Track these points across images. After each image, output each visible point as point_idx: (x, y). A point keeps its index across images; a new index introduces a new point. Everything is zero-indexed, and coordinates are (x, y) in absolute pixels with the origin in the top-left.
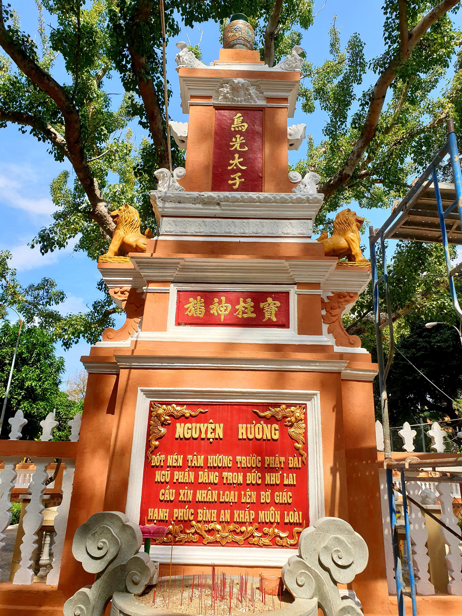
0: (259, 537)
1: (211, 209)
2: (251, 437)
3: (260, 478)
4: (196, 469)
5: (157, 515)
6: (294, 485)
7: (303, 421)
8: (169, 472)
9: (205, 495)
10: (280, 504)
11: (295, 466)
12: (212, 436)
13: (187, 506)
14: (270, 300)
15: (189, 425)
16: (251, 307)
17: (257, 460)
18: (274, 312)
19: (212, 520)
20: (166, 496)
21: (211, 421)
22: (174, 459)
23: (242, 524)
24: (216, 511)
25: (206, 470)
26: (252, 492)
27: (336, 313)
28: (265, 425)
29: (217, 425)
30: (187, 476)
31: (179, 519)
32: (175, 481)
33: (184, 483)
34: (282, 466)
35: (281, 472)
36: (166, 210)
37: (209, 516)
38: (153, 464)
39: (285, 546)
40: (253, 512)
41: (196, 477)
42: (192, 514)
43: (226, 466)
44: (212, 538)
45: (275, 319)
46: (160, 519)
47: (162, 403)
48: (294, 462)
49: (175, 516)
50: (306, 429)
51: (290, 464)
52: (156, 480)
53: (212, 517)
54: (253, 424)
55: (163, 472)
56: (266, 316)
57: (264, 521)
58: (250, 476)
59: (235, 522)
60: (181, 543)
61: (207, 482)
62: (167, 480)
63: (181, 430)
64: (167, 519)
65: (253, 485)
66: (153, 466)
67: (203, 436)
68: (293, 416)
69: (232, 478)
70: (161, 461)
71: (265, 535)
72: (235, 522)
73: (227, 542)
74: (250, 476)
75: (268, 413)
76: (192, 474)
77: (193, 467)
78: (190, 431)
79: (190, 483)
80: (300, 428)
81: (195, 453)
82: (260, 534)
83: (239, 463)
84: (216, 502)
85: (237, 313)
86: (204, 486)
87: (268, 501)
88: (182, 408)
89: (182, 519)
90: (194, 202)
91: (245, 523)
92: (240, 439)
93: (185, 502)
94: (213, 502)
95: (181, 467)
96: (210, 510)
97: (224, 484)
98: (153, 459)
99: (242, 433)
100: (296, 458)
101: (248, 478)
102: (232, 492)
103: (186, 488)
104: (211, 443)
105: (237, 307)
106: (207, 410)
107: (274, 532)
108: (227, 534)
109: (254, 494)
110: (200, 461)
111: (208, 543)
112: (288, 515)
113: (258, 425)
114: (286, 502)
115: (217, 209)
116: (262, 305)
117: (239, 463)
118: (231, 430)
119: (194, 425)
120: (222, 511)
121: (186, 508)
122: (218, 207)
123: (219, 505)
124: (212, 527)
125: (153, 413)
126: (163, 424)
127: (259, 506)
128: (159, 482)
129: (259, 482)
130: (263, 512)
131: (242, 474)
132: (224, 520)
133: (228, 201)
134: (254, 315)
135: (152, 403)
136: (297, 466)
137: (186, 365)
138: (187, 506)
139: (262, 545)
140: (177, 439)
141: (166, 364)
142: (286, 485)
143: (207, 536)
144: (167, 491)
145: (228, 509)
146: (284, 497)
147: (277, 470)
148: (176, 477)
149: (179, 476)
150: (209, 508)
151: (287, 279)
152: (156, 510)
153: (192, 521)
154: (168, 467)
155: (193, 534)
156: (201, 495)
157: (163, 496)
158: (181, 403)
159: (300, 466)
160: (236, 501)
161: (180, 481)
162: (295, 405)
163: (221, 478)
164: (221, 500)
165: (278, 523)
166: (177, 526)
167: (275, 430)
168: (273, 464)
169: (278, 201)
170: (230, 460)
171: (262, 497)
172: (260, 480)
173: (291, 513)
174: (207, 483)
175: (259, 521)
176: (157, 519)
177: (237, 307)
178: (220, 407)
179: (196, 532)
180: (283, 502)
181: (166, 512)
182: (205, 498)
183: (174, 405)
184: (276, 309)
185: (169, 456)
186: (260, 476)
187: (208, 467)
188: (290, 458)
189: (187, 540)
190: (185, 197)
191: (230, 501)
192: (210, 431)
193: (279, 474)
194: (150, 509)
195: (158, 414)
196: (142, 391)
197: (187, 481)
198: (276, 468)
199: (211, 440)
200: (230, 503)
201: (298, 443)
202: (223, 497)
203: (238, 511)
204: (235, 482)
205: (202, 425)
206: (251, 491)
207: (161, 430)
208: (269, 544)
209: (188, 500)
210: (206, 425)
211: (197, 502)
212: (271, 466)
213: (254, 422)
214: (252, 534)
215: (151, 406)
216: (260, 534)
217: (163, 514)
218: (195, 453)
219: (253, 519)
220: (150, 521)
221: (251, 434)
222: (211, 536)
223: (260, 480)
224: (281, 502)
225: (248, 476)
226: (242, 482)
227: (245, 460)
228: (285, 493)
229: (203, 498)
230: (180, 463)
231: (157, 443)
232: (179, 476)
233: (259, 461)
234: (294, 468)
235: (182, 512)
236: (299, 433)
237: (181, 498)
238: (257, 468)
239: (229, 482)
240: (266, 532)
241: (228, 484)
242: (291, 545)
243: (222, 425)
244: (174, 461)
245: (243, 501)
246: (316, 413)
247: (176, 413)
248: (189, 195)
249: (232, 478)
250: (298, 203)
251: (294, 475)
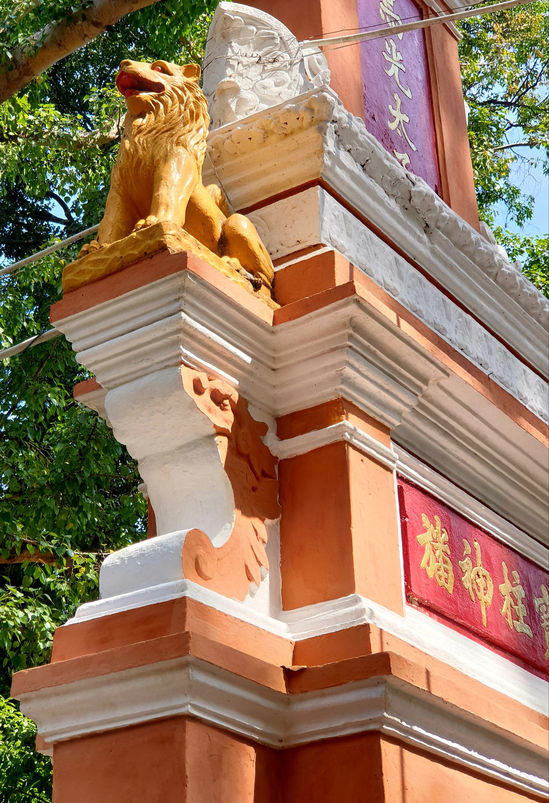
1: (414, 234)
36: (338, 170)
90: (389, 189)
122: (425, 237)
133: (448, 234)
190: (380, 161)
248: (388, 159)
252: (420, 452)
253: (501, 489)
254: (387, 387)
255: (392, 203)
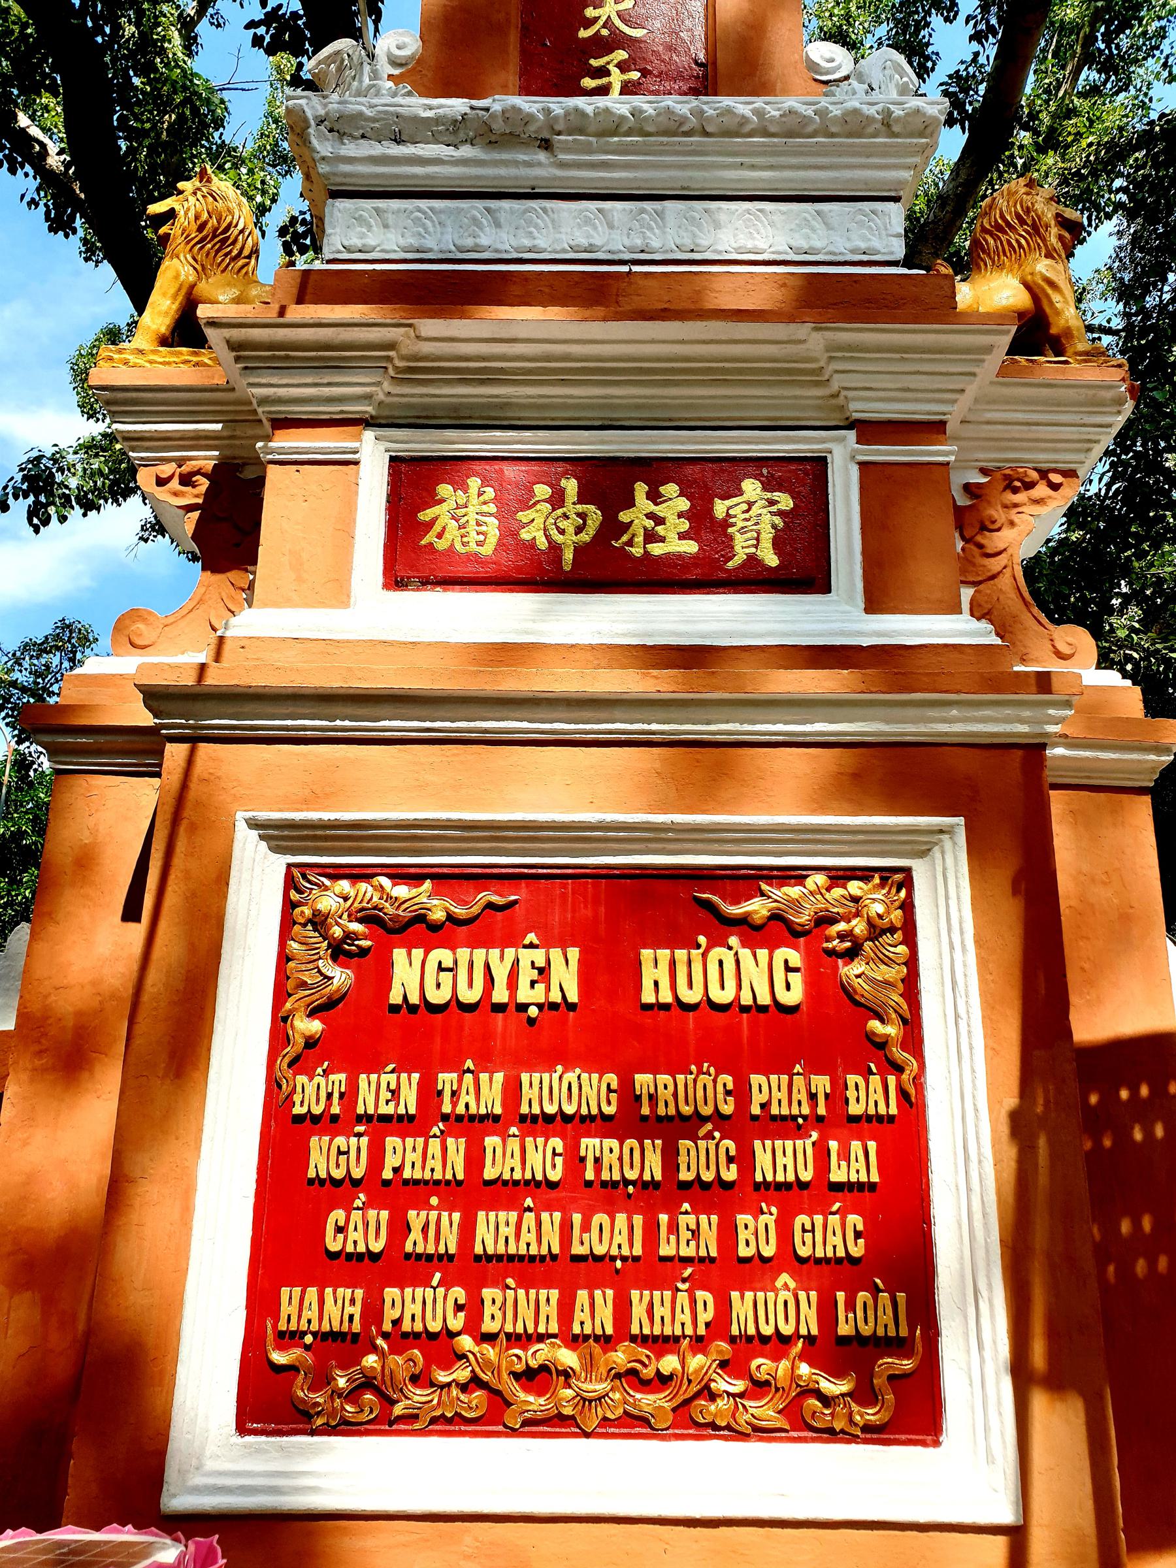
0: (734, 1395)
1: (516, 163)
2: (692, 996)
3: (730, 1160)
4: (474, 1126)
5: (313, 1314)
6: (872, 1186)
7: (899, 936)
8: (364, 1140)
9: (510, 1231)
10: (818, 1261)
11: (871, 1111)
12: (538, 994)
13: (438, 1276)
14: (751, 488)
15: (442, 955)
16: (680, 515)
17: (720, 1089)
18: (767, 536)
19: (541, 1329)
20: (352, 1235)
21: (531, 937)
22: (386, 1090)
23: (663, 1344)
24: (555, 1294)
25: (514, 1130)
26: (703, 1218)
27: (1001, 546)
28: (745, 954)
29: (556, 954)
30: (438, 1155)
31: (406, 1326)
32: (387, 1174)
33: (426, 1182)
34: (822, 1110)
35: (815, 1135)
37: (526, 1313)
38: (298, 1110)
39: (842, 1431)
40: (709, 1297)
41: (475, 1159)
42: (459, 1308)
43: (594, 1111)
44: (542, 1401)
45: (772, 560)
46: (326, 1327)
47: (336, 873)
48: (868, 1095)
49: (390, 1314)
50: (912, 963)
51: (852, 1101)
52: (311, 1174)
53: (542, 1318)
54: (699, 946)
55: (340, 1141)
56: (738, 548)
57: (751, 1331)
58: (693, 1153)
59: (633, 1339)
60: (417, 1426)
61: (517, 1176)
62: (358, 1173)
63: (411, 974)
64: (357, 1327)
65: (705, 1186)
66: (299, 1119)
67: (500, 995)
68: (857, 914)
69: (620, 1159)
70: (330, 1096)
71: (759, 1388)
72: (633, 1339)
73: (605, 1419)
74: (693, 1153)
75: (757, 908)
76: (457, 1149)
77: (459, 1118)
78: (446, 977)
79: (448, 1182)
80: (888, 962)
81: (469, 1064)
82: (739, 1386)
83: (645, 1100)
84: (554, 1257)
85: (625, 538)
86: (506, 1193)
87: (769, 1251)
88: (415, 892)
89: (419, 1327)
90: (451, 139)
91: (677, 1339)
92: (648, 1007)
93: (429, 1257)
94: (543, 1258)
95: (411, 1118)
96: (532, 1292)
97: (589, 1184)
98: (299, 1089)
99: (656, 983)
100: (875, 1080)
101: (682, 1160)
102: (621, 1218)
103: (434, 1201)
104: (531, 1021)
105: (624, 517)
106: (513, 898)
107: (794, 1377)
108: (601, 1387)
109: (709, 1224)
110: (486, 1093)
111: (525, 1423)
112: (850, 1306)
113: (717, 952)
114: (841, 1253)
115: (540, 164)
116: (720, 508)
117: (645, 1100)
118: (609, 971)
119: (463, 953)
120: (582, 1295)
121: (435, 1283)
122: (542, 156)
123: (565, 1271)
124: (541, 1358)
125: (298, 910)
126: (338, 952)
127: (728, 1272)
128: (322, 1182)
129: (731, 1174)
130: (749, 1295)
131: (658, 1142)
132: (588, 1330)
133: (581, 132)
134: (690, 547)
135: (296, 872)
136: (882, 1110)
137: (428, 724)
138: (438, 1276)
139: (749, 1430)
140: (395, 1008)
141: (347, 723)
142: (838, 1187)
143: (522, 1396)
144: (356, 1216)
145: (602, 1285)
146: (834, 1234)
147: (799, 1127)
148: (391, 1161)
149: (404, 1156)
150: (526, 1283)
151: (819, 408)
152: (312, 1292)
153: (459, 1334)
154: (360, 1119)
155: (464, 1388)
156: (494, 1231)
157: (341, 1236)
158: (412, 870)
159: (894, 1110)
160: (638, 1251)
161: (407, 1174)
162: (863, 874)
163: (575, 1161)
164: (577, 1249)
165: (809, 1339)
166: (400, 1354)
167: (788, 969)
168: (785, 1103)
169: (772, 129)
170: (609, 1090)
171: (743, 1235)
172: (733, 1167)
173: (863, 1296)
174: (516, 1183)
175: (735, 1331)
176: (314, 1327)
177: (624, 517)
178: (565, 886)
179: (475, 1382)
180: (830, 1254)
181: (353, 1302)
182: (512, 1240)
183: (385, 882)
184: (778, 520)
185: (363, 1077)
186: (733, 1153)
187: (523, 1118)
188: (852, 1079)
189: (438, 1413)
190: (416, 119)
191: (614, 1252)
192: (526, 975)
193: (809, 1142)
194: (285, 1291)
195: (316, 913)
196: (253, 824)
197: (438, 1176)
198: (795, 1118)
199: (533, 1011)
200: (613, 1259)
201: (882, 1021)
202: (586, 1236)
203: (646, 1293)
204: (632, 1175)
205: (495, 953)
206: (696, 1211)
207: (329, 974)
208: (778, 1425)
209: (442, 1250)
210: (510, 953)
211: (478, 1258)
212: (775, 1110)
213: (702, 940)
214: (707, 1387)
215: (290, 883)
216: (739, 1386)
217: (340, 1307)
218: (469, 1064)
219: (707, 1325)
220: (288, 1339)
221: (690, 986)
222: (540, 1394)
223: (733, 1167)
224: (819, 1253)
225: (683, 1152)
226: (658, 1176)
227: (671, 1088)
228: (834, 1220)
229: (502, 1241)
230: (410, 1101)
231: (315, 1026)
232: (404, 1156)
233: (728, 1093)
234: (869, 1118)
235: (419, 1300)
236: (887, 982)
237: (414, 1242)
238: (718, 1117)
239: (605, 1176)
240: (762, 1376)
241: (604, 1184)
242: (867, 1428)
243: (574, 953)
244: (385, 1095)
245: (666, 1250)
246: (953, 902)
247: (390, 910)
249: (620, 1159)
250: (850, 135)
251: (872, 1146)
252: (450, 418)
253: (635, 397)
254: (325, 381)
255: (466, 151)
